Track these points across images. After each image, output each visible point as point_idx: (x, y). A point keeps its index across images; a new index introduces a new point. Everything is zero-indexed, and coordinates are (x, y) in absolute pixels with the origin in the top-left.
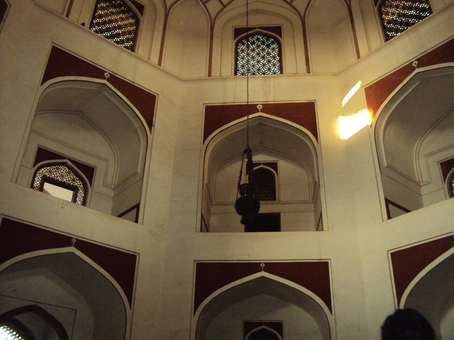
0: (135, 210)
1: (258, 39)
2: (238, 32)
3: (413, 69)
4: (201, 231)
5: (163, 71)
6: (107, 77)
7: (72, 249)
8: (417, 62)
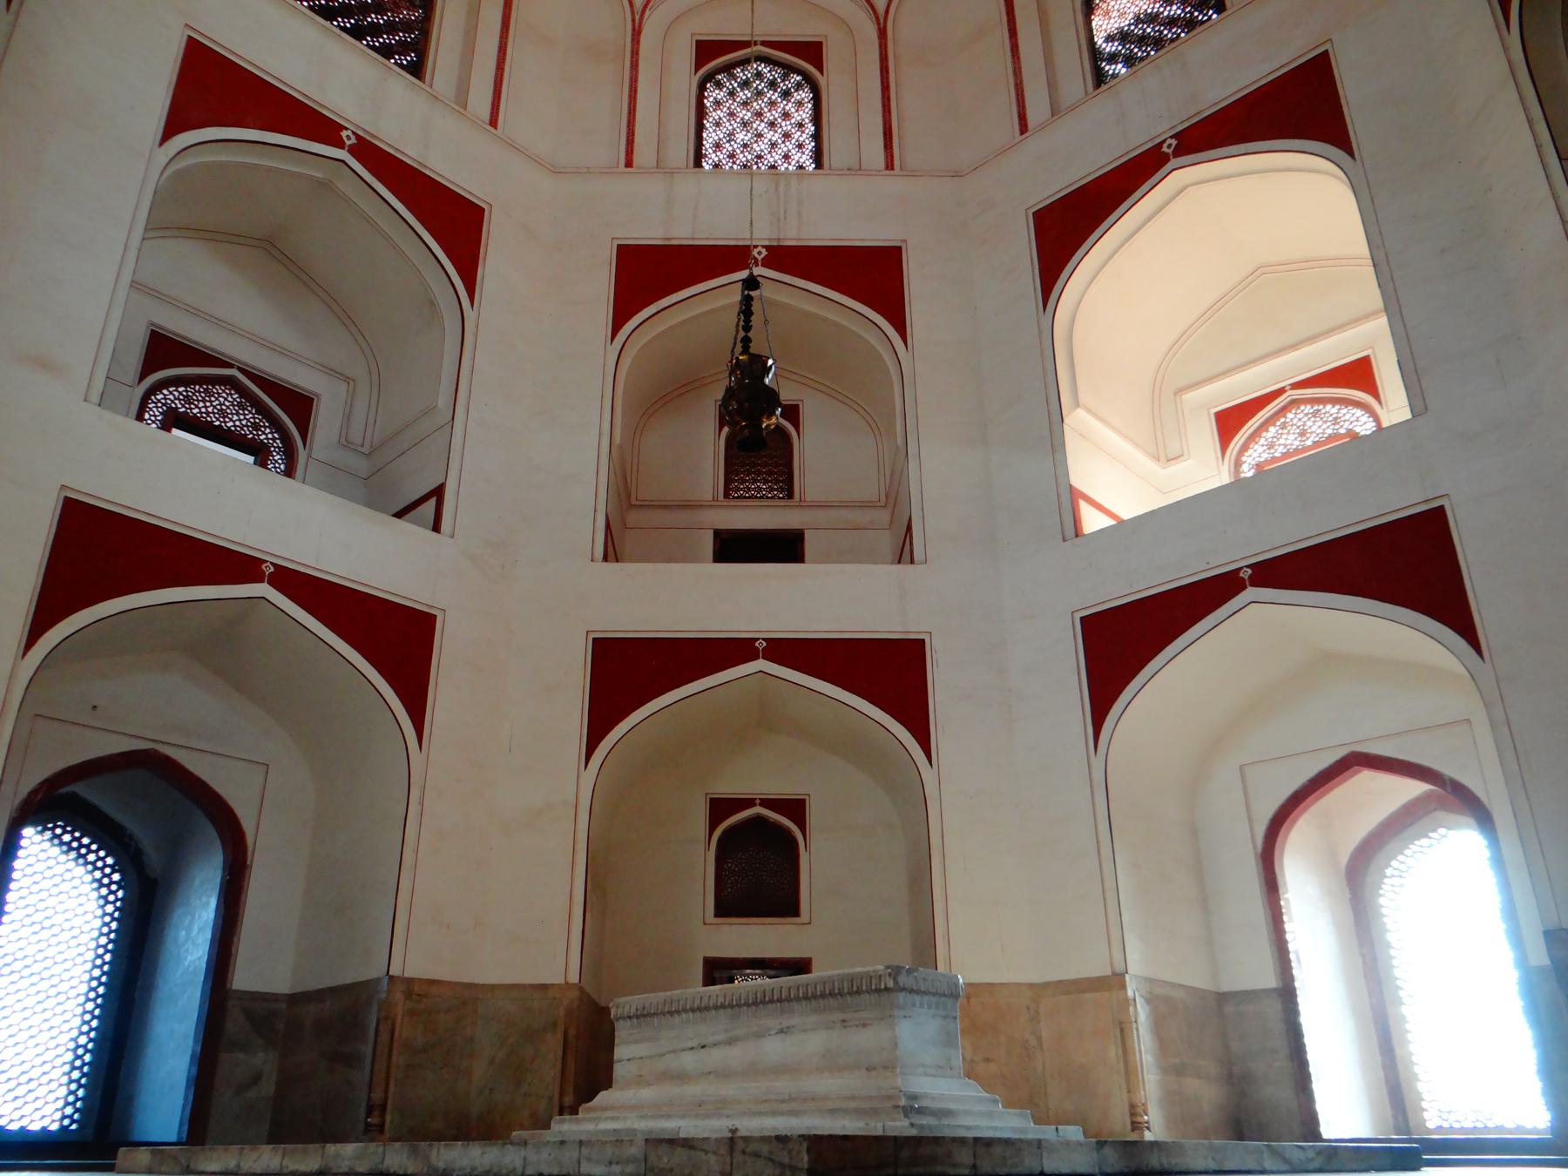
1: (759, 75)
2: (706, 50)
4: (605, 559)
6: (348, 143)
7: (263, 589)
8: (1174, 142)
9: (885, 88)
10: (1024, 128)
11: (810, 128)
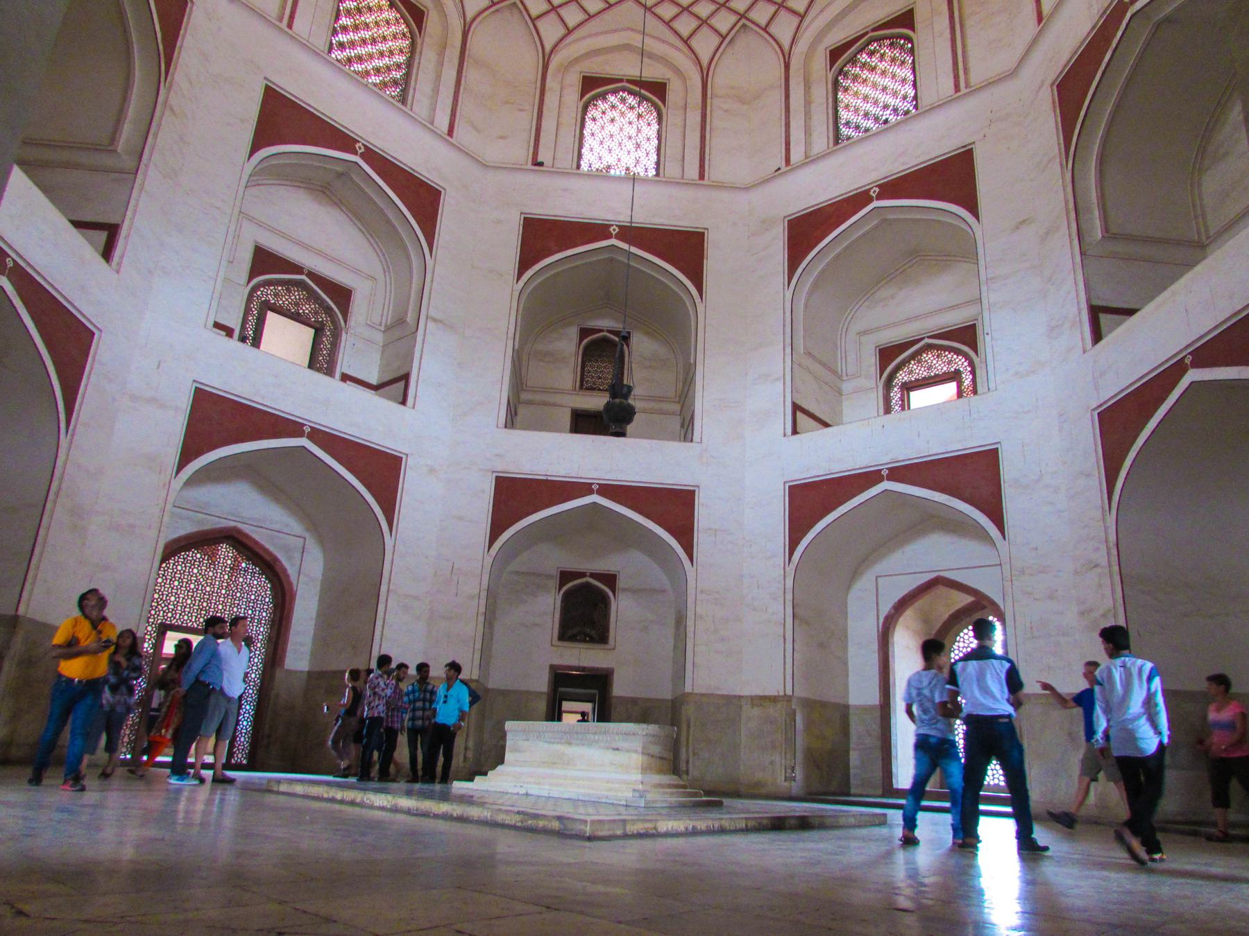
3: (870, 200)
5: (453, 145)
9: (703, 137)
11: (654, 157)
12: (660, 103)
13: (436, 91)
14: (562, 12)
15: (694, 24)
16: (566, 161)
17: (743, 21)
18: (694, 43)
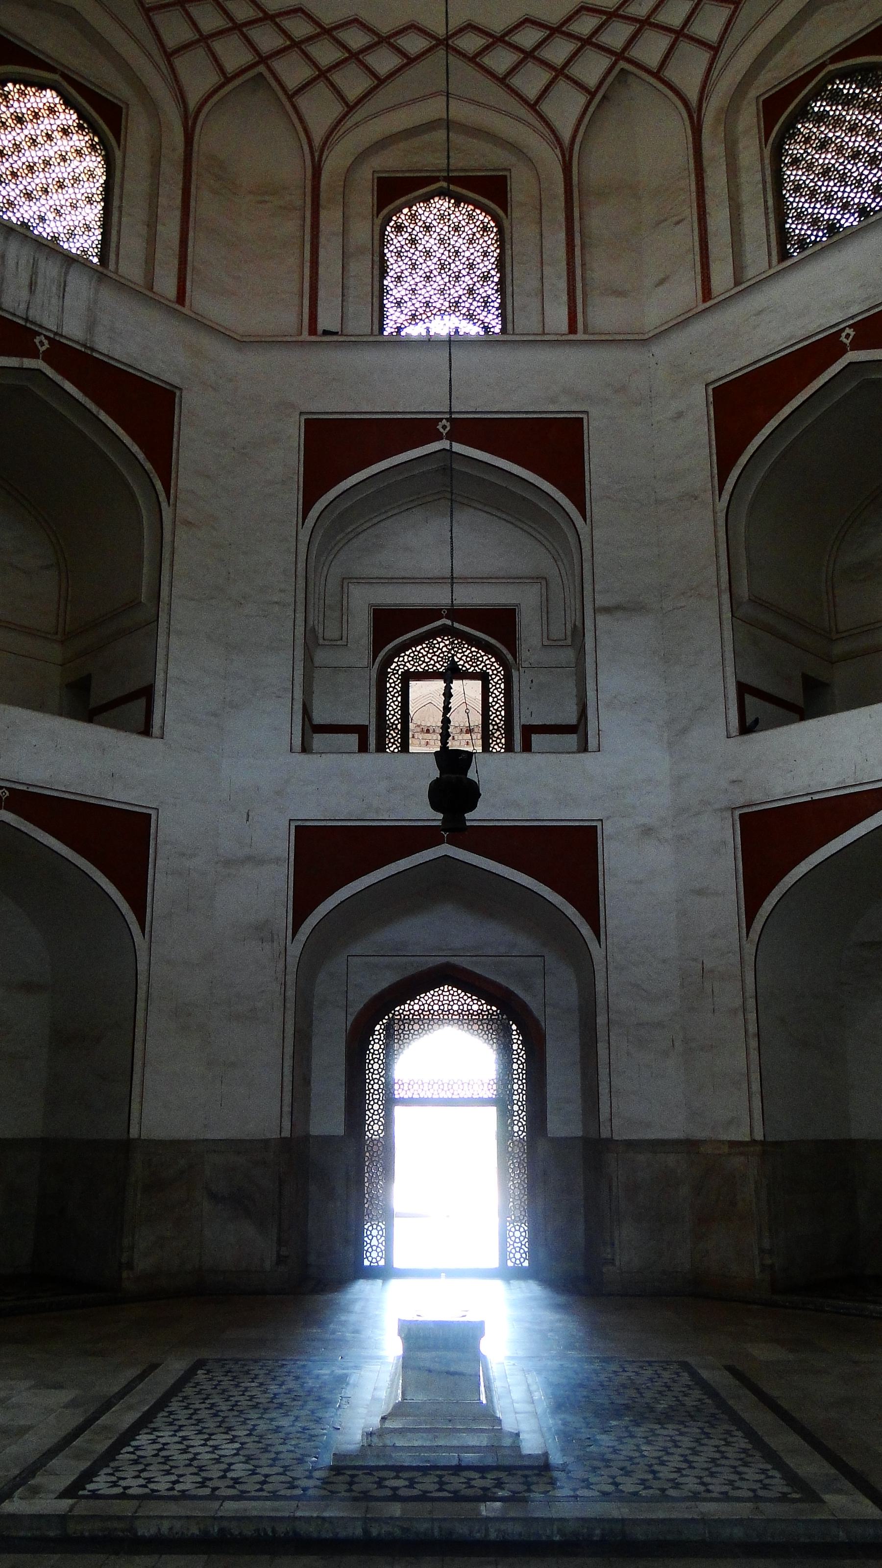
0: (142, 702)
6: (42, 349)
8: (852, 332)
10: (707, 293)
12: (500, 212)
13: (152, 223)
14: (336, 77)
15: (545, 76)
16: (361, 324)
17: (622, 64)
18: (545, 107)
